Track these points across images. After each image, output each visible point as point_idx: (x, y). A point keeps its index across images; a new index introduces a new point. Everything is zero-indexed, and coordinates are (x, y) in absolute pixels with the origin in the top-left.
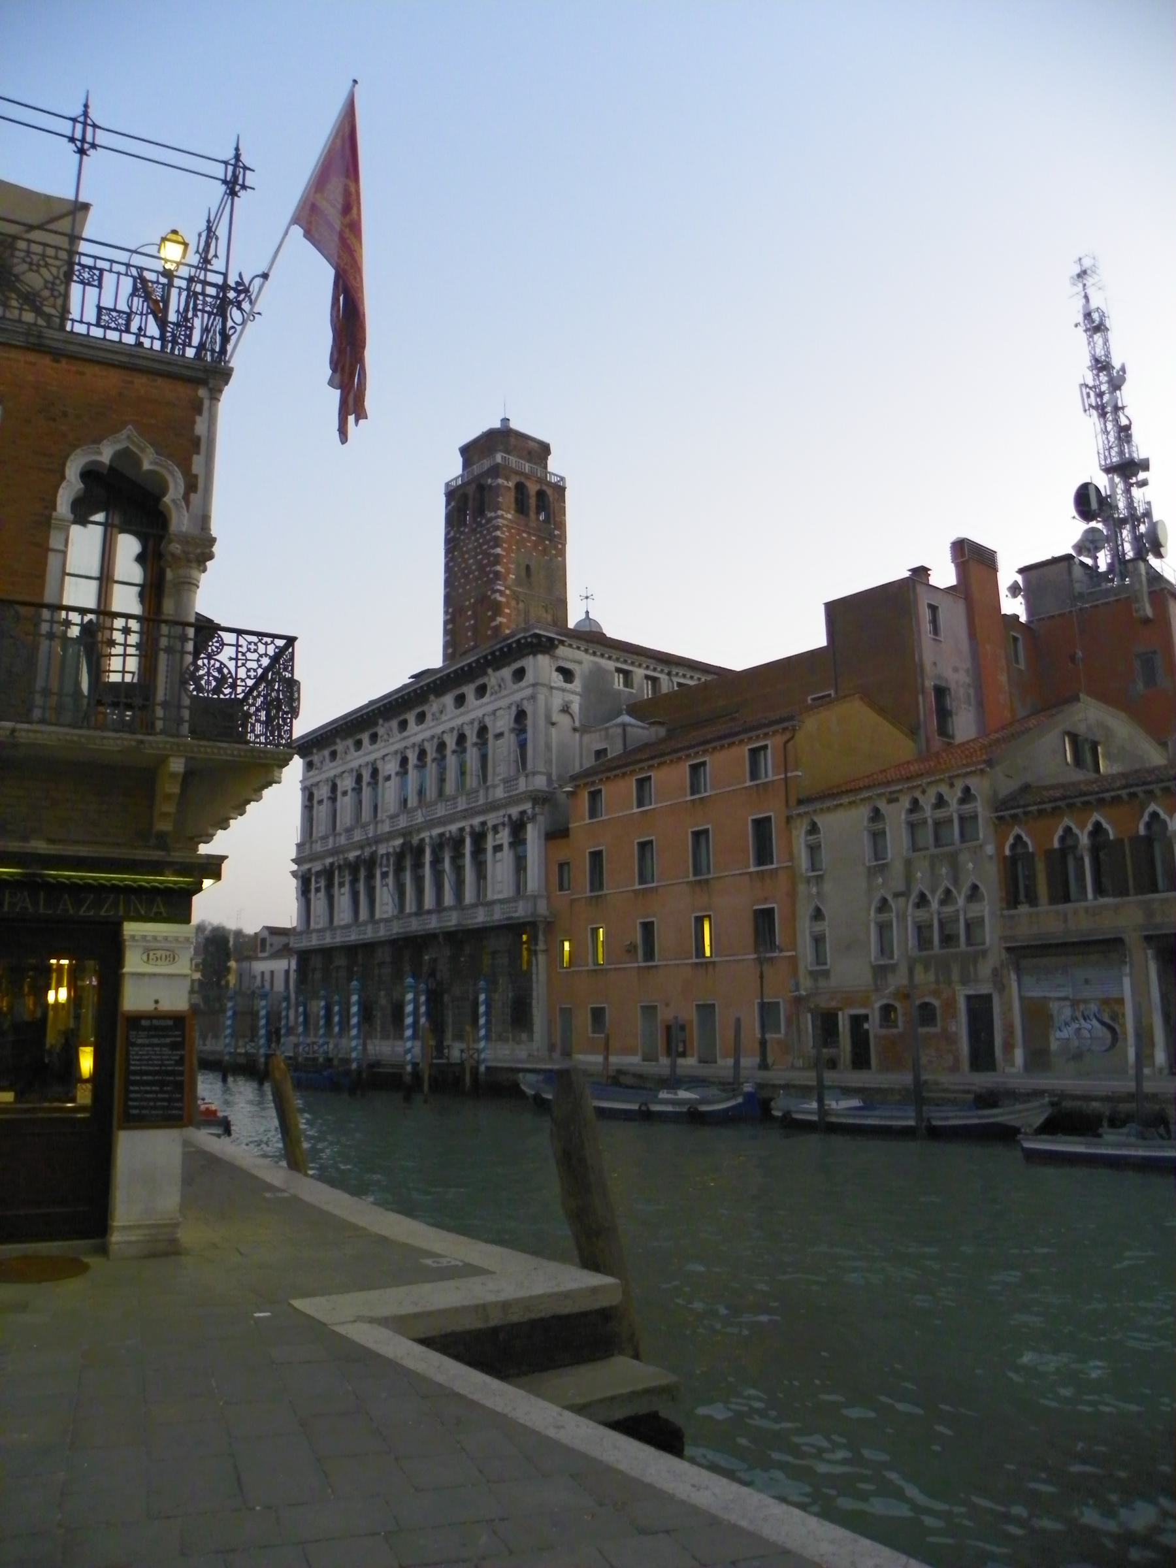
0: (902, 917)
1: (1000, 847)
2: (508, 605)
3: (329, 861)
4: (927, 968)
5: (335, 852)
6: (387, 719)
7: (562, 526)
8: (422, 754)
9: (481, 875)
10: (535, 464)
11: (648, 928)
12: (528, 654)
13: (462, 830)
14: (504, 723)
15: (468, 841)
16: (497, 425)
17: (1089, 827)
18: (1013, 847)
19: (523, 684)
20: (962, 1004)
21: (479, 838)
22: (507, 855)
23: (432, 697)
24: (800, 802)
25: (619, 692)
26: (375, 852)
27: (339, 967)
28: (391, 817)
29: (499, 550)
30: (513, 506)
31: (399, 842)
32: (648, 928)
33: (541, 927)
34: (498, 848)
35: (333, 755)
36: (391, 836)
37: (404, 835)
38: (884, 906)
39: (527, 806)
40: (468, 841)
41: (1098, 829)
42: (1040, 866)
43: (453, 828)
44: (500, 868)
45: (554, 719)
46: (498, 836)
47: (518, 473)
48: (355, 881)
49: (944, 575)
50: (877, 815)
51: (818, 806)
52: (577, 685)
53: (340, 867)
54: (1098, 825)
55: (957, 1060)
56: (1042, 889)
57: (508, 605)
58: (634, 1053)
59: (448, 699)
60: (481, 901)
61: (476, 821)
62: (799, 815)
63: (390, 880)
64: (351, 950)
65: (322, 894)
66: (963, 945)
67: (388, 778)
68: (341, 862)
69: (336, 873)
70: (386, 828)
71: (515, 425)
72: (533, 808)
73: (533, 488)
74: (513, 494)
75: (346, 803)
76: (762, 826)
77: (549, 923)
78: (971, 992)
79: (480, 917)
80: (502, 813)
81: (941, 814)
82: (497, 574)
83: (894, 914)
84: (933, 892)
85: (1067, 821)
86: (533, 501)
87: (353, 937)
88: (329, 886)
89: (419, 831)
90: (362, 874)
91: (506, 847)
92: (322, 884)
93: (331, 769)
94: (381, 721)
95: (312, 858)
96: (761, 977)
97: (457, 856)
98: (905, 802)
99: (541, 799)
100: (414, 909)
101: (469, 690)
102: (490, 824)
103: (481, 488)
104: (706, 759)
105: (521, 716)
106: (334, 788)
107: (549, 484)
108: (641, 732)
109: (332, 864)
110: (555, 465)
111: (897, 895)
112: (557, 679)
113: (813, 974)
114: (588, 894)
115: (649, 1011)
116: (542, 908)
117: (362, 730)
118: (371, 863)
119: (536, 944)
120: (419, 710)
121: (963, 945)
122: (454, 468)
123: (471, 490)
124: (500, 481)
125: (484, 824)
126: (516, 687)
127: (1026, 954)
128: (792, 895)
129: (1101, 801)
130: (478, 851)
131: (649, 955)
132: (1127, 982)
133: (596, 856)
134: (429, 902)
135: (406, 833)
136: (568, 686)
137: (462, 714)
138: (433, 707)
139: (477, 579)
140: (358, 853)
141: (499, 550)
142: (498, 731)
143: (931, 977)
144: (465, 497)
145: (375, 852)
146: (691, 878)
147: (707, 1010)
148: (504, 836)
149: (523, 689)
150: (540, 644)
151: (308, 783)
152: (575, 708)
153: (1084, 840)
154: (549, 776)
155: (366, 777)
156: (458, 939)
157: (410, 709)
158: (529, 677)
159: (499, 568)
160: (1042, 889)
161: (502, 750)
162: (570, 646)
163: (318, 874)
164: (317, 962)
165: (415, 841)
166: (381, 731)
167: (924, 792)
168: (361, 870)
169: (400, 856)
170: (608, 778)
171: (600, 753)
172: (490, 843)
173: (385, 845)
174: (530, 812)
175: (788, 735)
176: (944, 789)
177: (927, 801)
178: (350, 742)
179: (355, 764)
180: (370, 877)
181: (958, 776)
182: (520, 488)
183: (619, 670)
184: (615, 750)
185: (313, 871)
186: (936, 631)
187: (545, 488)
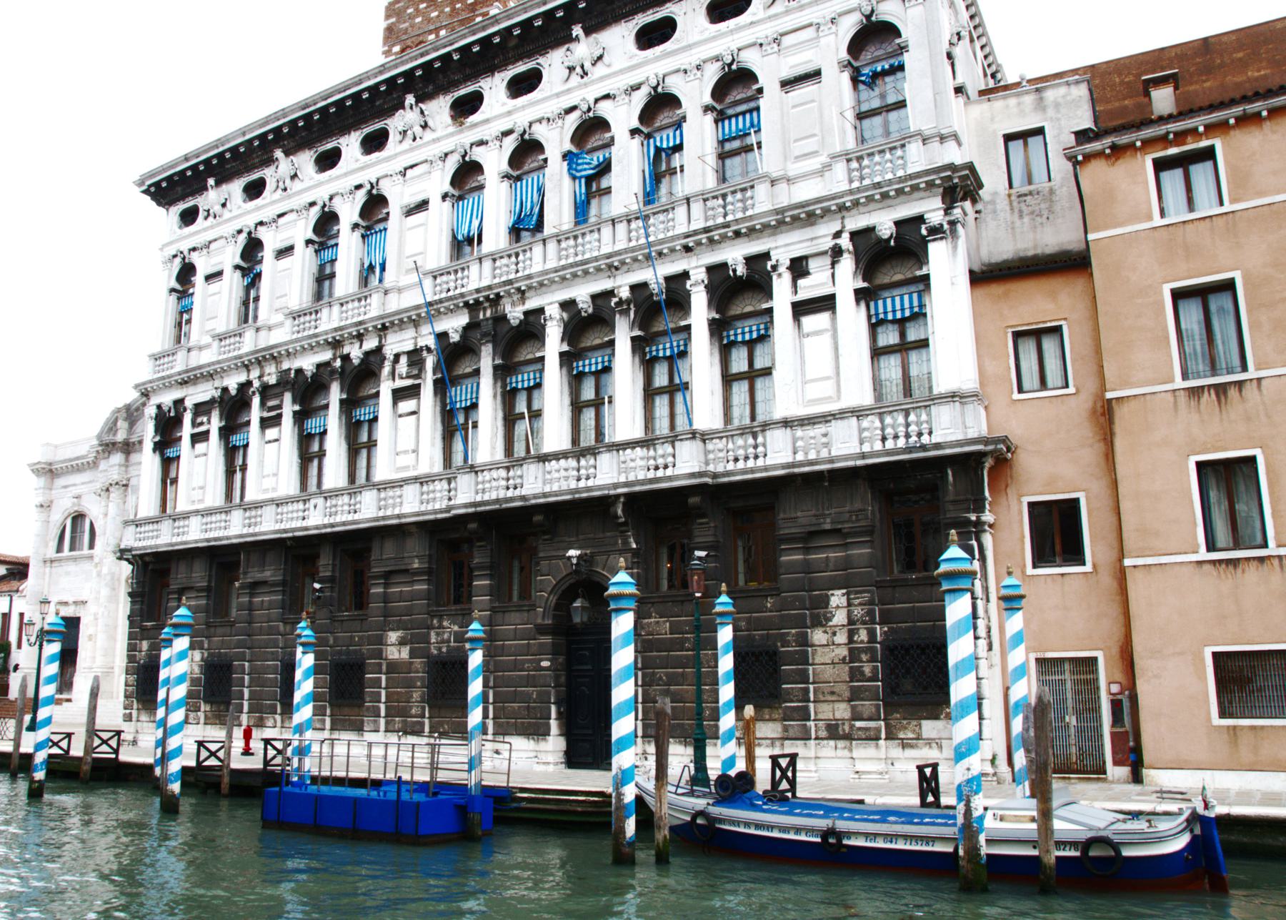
21: (740, 292)
23: (577, 30)
26: (379, 349)
31: (463, 319)
36: (433, 310)
39: (932, 209)
46: (801, 282)
53: (266, 391)
64: (298, 552)
65: (214, 445)
68: (272, 380)
69: (256, 401)
72: (947, 211)
79: (778, 453)
87: (317, 518)
90: (335, 394)
91: (845, 300)
92: (215, 423)
94: (410, 99)
106: (252, 248)
118: (360, 378)
119: (980, 509)
120: (521, 68)
140: (326, 356)
145: (379, 349)
151: (185, 246)
157: (491, 70)
163: (201, 409)
165: (515, 313)
169: (454, 356)
173: (410, 333)
185: (189, 403)
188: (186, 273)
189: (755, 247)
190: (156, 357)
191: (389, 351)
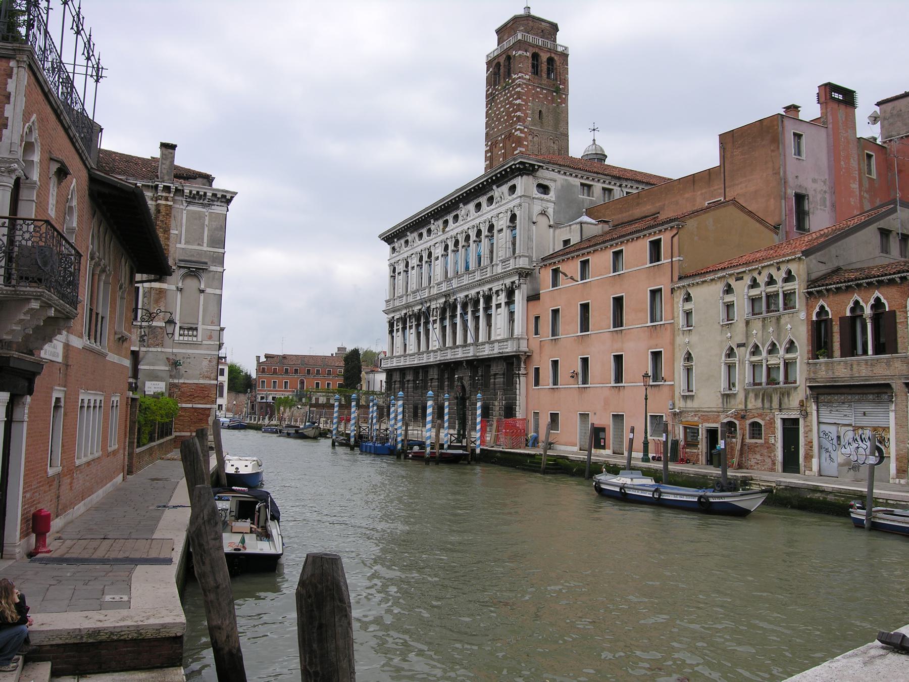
0: (742, 362)
1: (809, 315)
2: (526, 139)
3: (404, 311)
4: (756, 396)
5: (408, 306)
6: (436, 220)
7: (565, 82)
8: (457, 243)
9: (489, 324)
10: (547, 39)
11: (585, 361)
12: (518, 176)
13: (478, 293)
14: (503, 222)
15: (482, 301)
16: (521, 12)
17: (872, 302)
18: (818, 314)
19: (514, 196)
20: (779, 425)
21: (488, 299)
22: (503, 310)
23: (461, 205)
24: (680, 278)
25: (583, 201)
27: (408, 381)
28: (438, 284)
29: (518, 102)
30: (530, 68)
31: (443, 300)
32: (585, 361)
33: (523, 358)
34: (498, 306)
35: (407, 242)
37: (445, 296)
38: (731, 353)
39: (516, 278)
40: (482, 301)
41: (878, 304)
42: (836, 329)
43: (473, 292)
44: (500, 317)
45: (534, 220)
47: (533, 46)
48: (418, 325)
49: (811, 110)
50: (729, 290)
51: (690, 281)
52: (552, 195)
53: (410, 316)
54: (878, 300)
55: (774, 464)
56: (837, 346)
57: (526, 139)
58: (575, 445)
59: (471, 206)
60: (490, 342)
61: (486, 288)
62: (679, 288)
63: (437, 325)
64: (416, 370)
66: (781, 385)
67: (437, 258)
70: (434, 291)
71: (534, 12)
73: (544, 57)
74: (530, 61)
75: (413, 274)
76: (655, 293)
77: (529, 356)
78: (786, 417)
79: (486, 352)
80: (501, 282)
81: (771, 289)
82: (519, 118)
83: (737, 359)
84: (763, 346)
85: (856, 297)
86: (544, 66)
87: (416, 362)
88: (404, 329)
89: (454, 293)
91: (503, 305)
92: (400, 327)
93: (405, 252)
94: (432, 221)
95: (395, 310)
96: (646, 399)
97: (475, 311)
98: (747, 280)
99: (525, 274)
100: (451, 345)
101: (483, 200)
102: (494, 290)
103: (509, 58)
104: (623, 248)
105: (513, 218)
107: (556, 52)
108: (593, 228)
109: (406, 314)
110: (562, 39)
111: (739, 346)
112: (535, 193)
113: (685, 398)
114: (551, 338)
115: (584, 416)
116: (524, 347)
117: (423, 227)
118: (427, 314)
121: (781, 385)
122: (491, 45)
123: (502, 60)
124: (520, 52)
125: (491, 289)
126: (510, 198)
127: (823, 393)
128: (673, 343)
129: (880, 283)
130: (487, 308)
131: (585, 381)
132: (892, 415)
133: (555, 312)
134: (459, 341)
135: (447, 295)
136: (545, 197)
137: (479, 216)
138: (462, 211)
139: (506, 121)
140: (420, 307)
141: (518, 102)
142: (500, 228)
143: (759, 404)
144: (498, 64)
146: (612, 329)
147: (618, 418)
148: (502, 298)
149: (514, 199)
150: (525, 168)
151: (393, 261)
152: (550, 211)
153: (868, 311)
154: (530, 258)
155: (425, 258)
156: (475, 364)
157: (449, 213)
158: (519, 191)
159: (518, 114)
160: (837, 346)
161: (502, 240)
162: (547, 169)
164: (396, 377)
165: (452, 300)
166: (433, 227)
167: (760, 273)
168: (421, 318)
169: (443, 311)
170: (563, 260)
171: (566, 242)
172: (494, 303)
174: (517, 282)
175: (675, 232)
176: (773, 271)
177: (762, 279)
178: (415, 235)
179: (418, 249)
180: (427, 323)
181: (783, 262)
182: (535, 56)
183: (582, 184)
184: (575, 239)
186: (799, 153)
187: (553, 55)
188: (394, 271)
189: (489, 286)
190: (387, 301)
191: (432, 307)
